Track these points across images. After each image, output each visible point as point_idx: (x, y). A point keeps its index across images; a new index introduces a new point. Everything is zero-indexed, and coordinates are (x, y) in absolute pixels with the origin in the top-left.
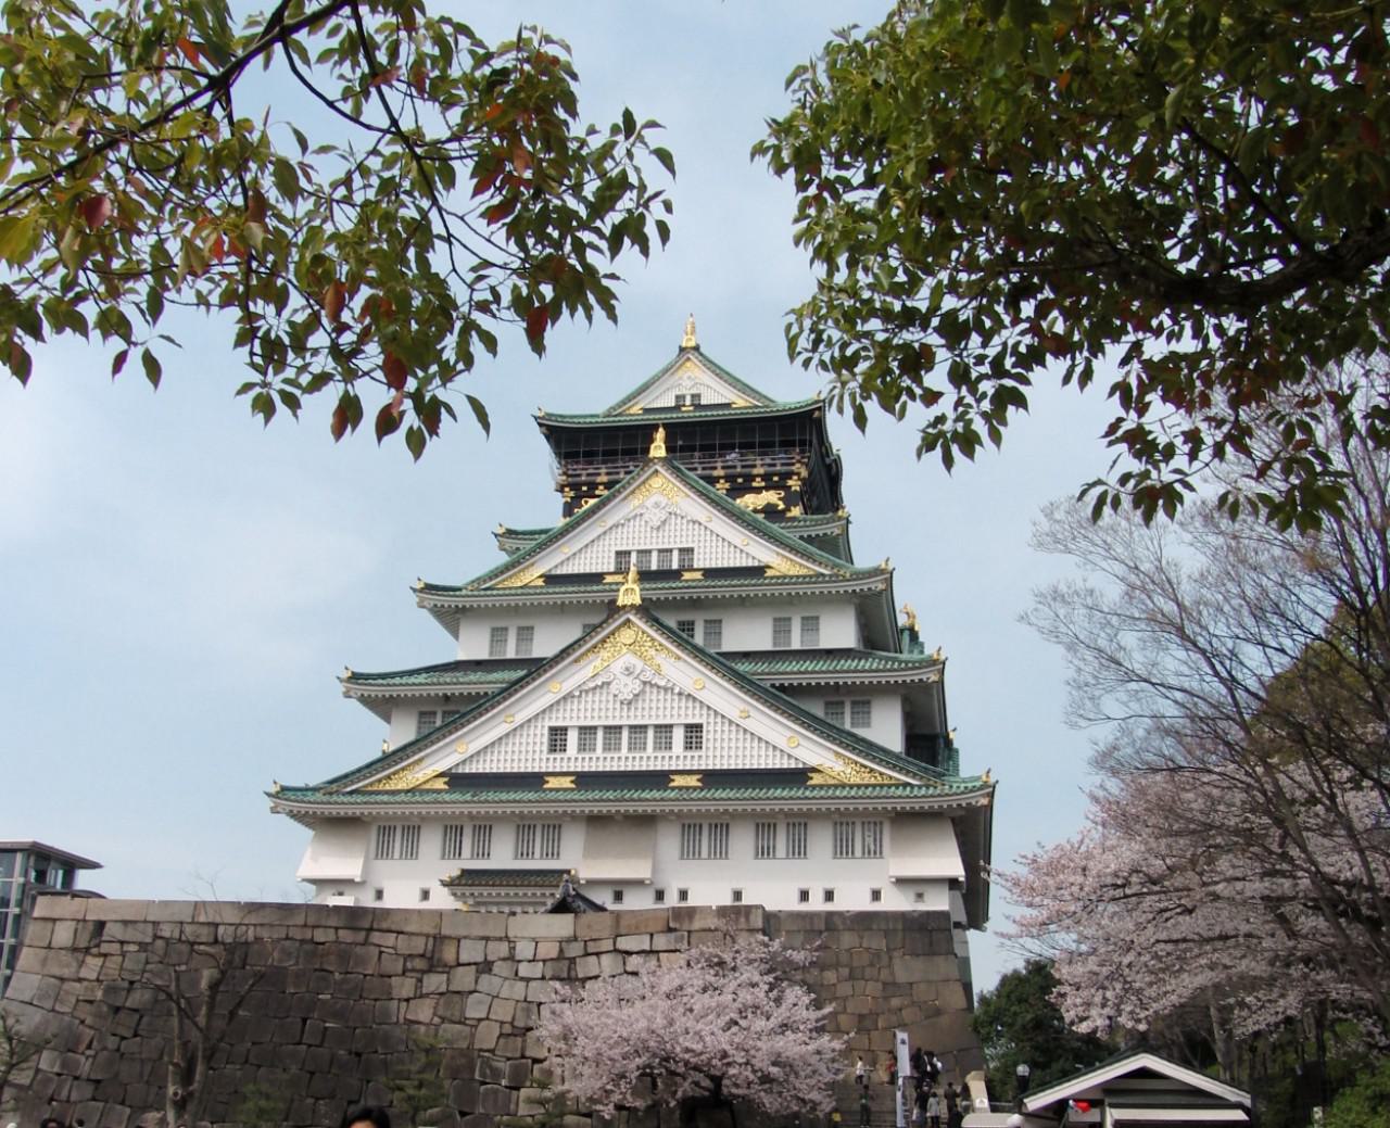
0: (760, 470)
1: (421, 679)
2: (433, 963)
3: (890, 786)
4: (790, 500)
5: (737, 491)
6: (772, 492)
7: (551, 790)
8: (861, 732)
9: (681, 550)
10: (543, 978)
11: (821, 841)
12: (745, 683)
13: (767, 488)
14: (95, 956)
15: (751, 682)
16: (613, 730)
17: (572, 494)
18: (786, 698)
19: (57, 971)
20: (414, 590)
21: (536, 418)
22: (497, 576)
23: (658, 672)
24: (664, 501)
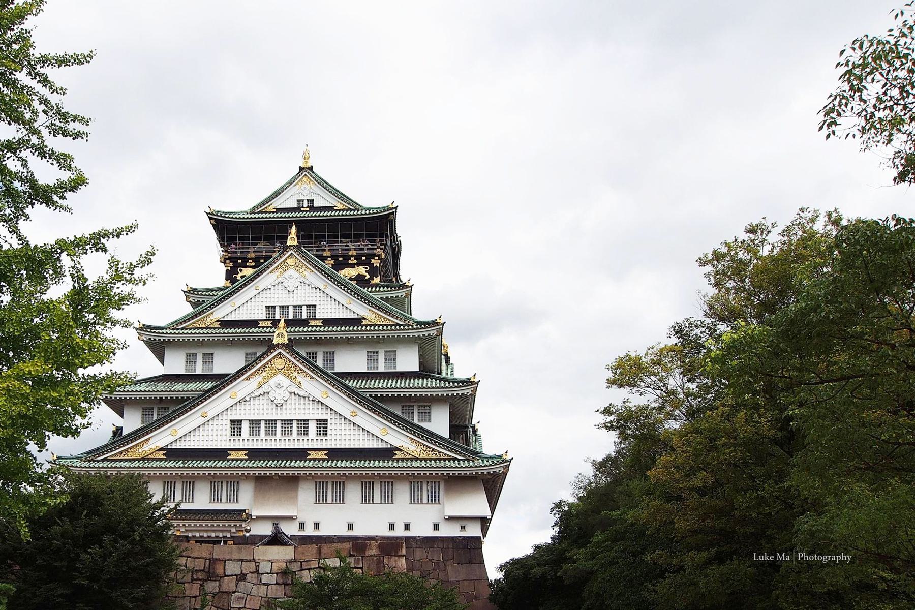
0: (355, 253)
1: (143, 387)
3: (445, 460)
4: (373, 272)
5: (338, 266)
6: (361, 267)
7: (233, 460)
8: (422, 425)
10: (277, 584)
11: (402, 493)
12: (353, 394)
13: (358, 264)
15: (357, 394)
16: (271, 423)
17: (231, 264)
18: (377, 405)
20: (137, 329)
22: (189, 320)
23: (299, 386)
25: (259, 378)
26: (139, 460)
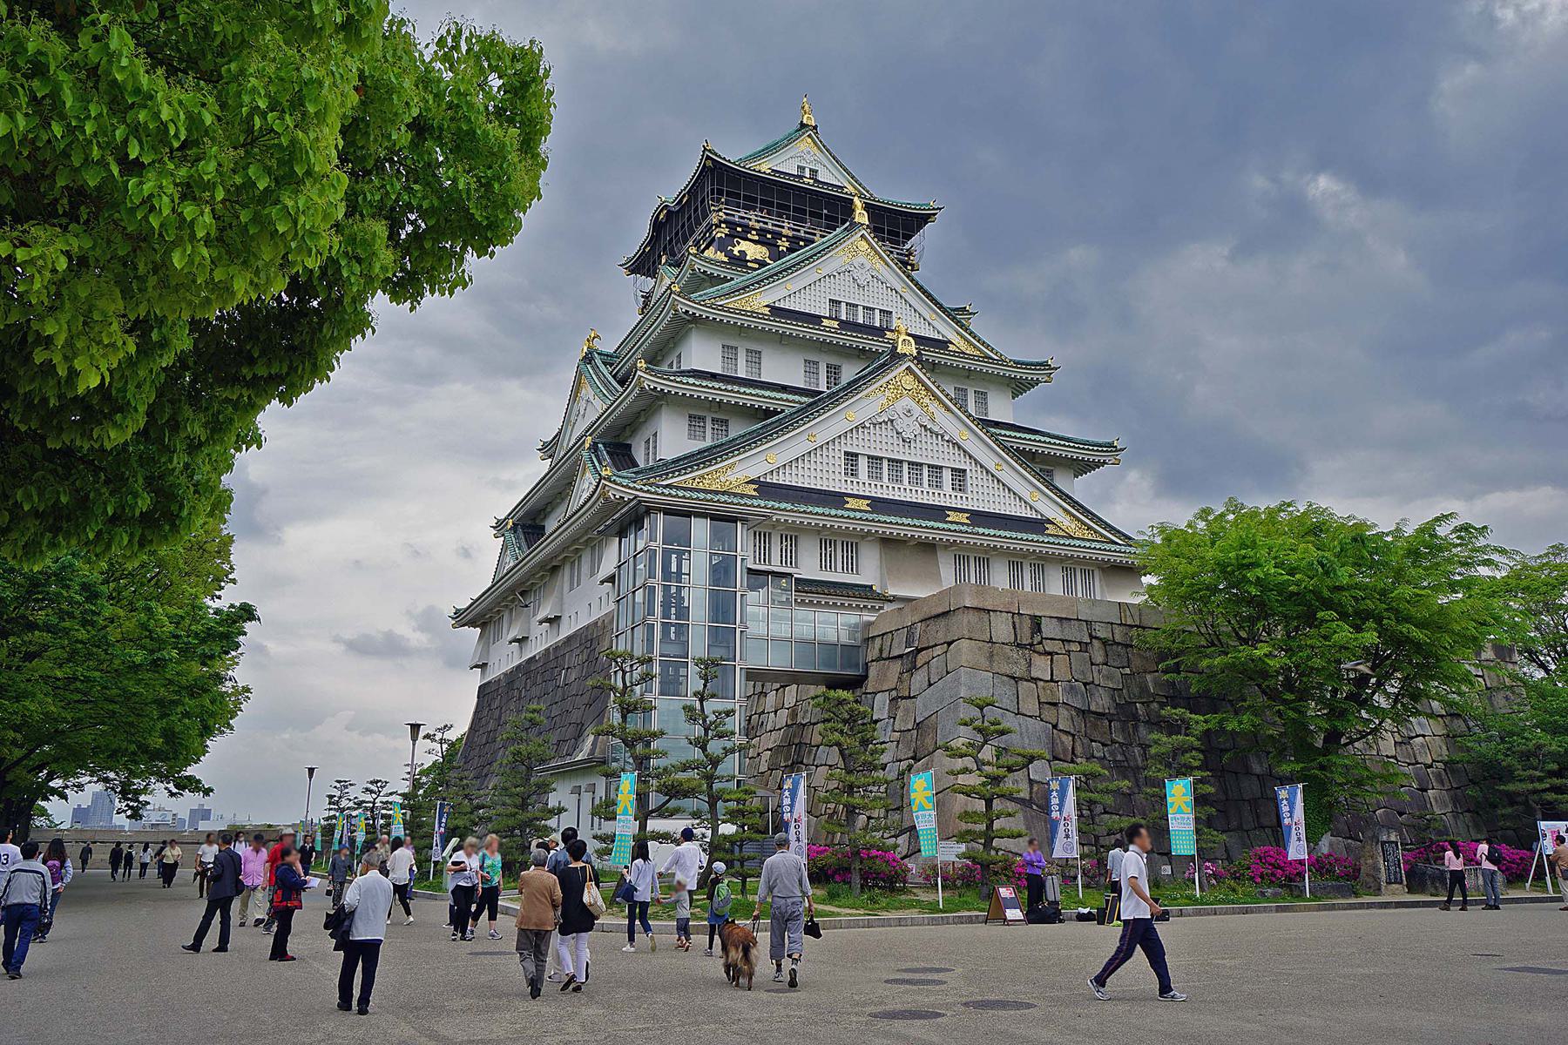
14: (1040, 654)
19: (1006, 669)
26: (724, 493)
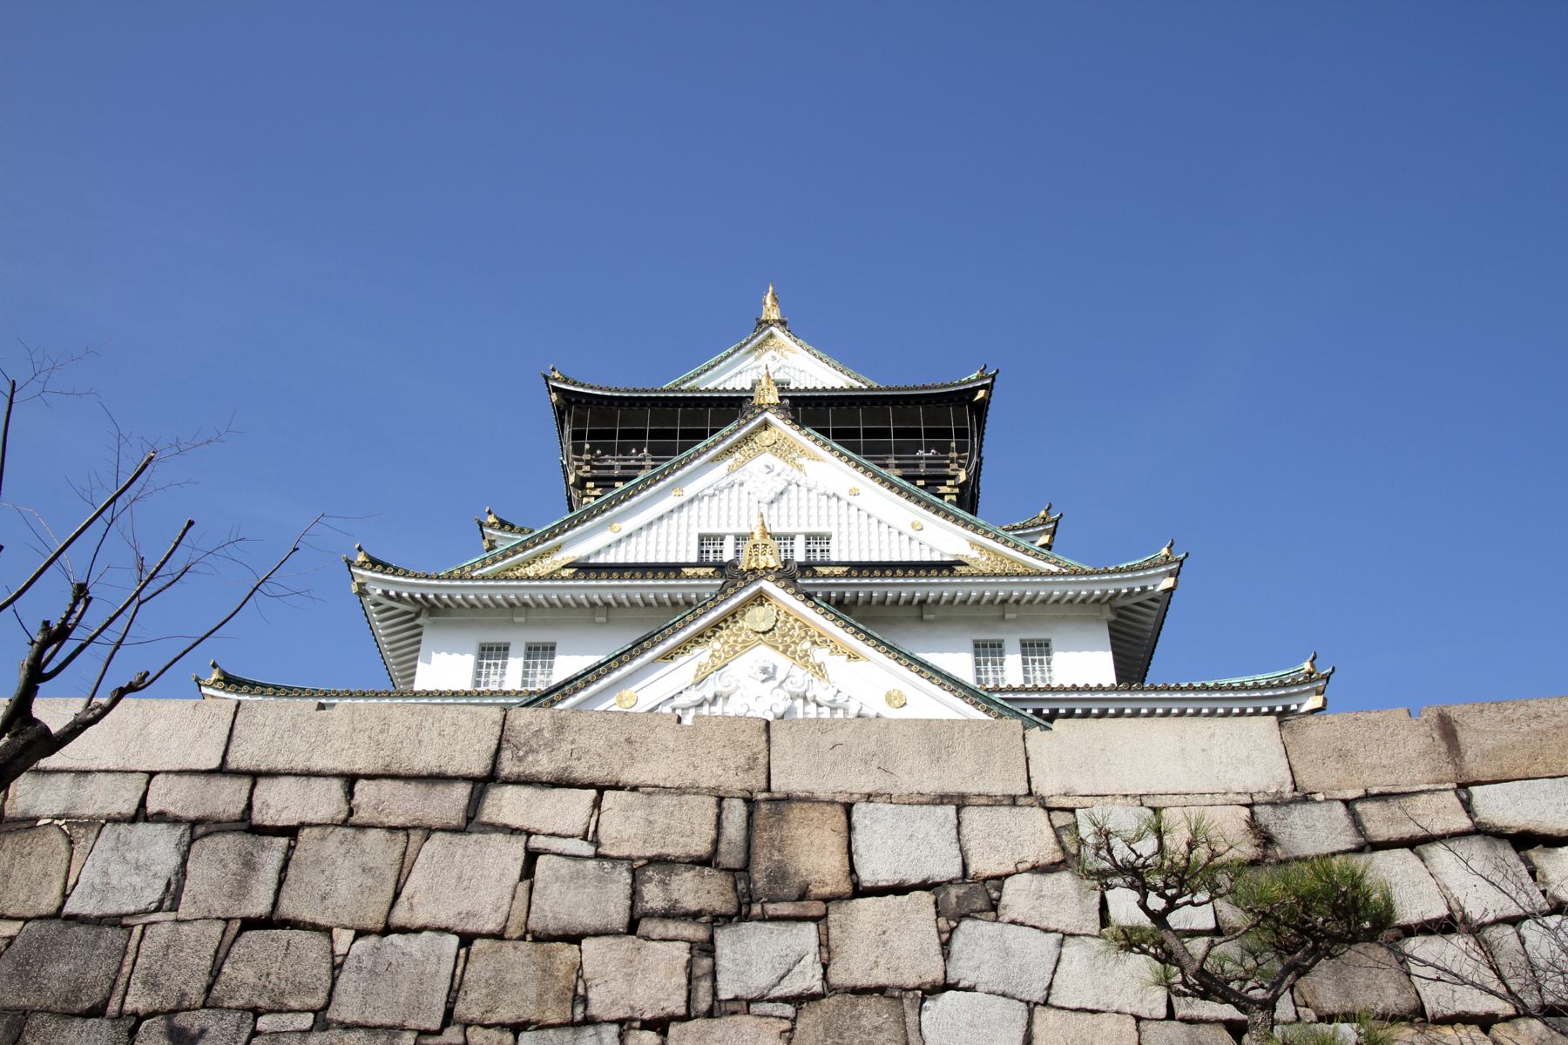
2: (752, 888)
9: (809, 537)
21: (546, 378)
24: (778, 464)
25: (701, 655)
